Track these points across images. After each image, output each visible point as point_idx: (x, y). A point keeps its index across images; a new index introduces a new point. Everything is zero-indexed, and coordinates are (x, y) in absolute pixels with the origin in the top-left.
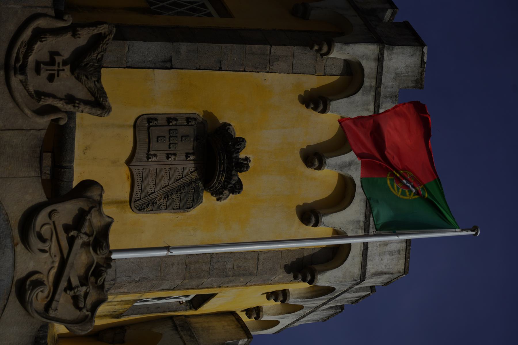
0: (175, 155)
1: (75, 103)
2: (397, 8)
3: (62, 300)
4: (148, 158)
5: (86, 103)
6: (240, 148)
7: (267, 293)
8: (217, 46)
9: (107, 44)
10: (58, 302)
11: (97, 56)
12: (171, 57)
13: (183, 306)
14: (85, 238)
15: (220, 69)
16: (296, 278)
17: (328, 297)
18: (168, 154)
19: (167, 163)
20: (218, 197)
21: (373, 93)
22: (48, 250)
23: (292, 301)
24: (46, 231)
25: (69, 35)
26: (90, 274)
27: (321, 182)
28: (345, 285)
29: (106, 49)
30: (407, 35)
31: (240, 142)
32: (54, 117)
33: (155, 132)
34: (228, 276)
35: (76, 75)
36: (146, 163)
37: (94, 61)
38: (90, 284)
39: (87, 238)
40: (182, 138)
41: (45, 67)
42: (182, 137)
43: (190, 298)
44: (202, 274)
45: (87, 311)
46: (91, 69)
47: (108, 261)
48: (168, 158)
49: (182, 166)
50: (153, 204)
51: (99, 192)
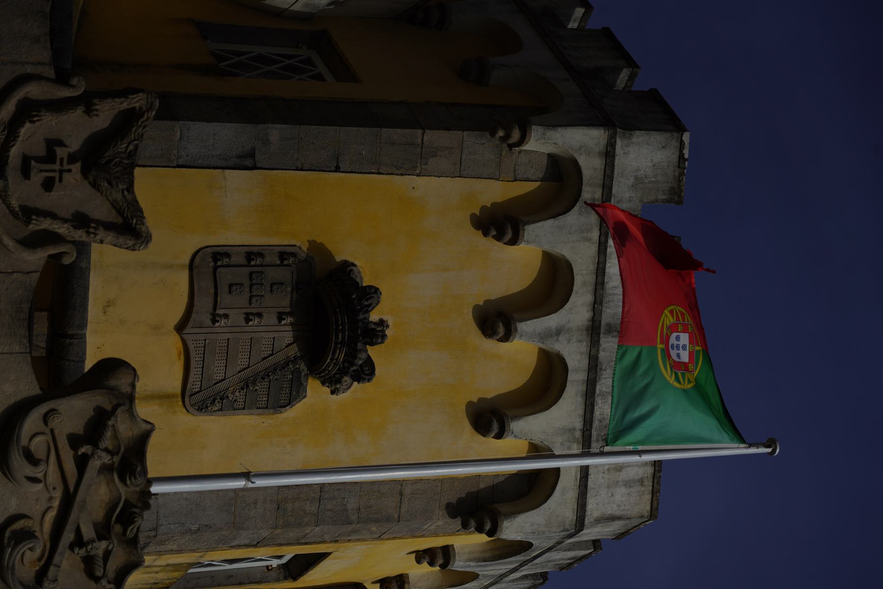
0: (260, 315)
1: (89, 227)
2: (638, 67)
3: (65, 565)
4: (214, 321)
5: (109, 227)
6: (370, 305)
7: (417, 552)
10: (59, 567)
11: (127, 147)
13: (272, 573)
14: (106, 459)
15: (337, 170)
16: (465, 526)
17: (521, 558)
18: (247, 314)
19: (246, 329)
20: (333, 387)
22: (42, 479)
23: (459, 565)
24: (38, 445)
25: (80, 111)
26: (114, 519)
27: (509, 363)
29: (142, 135)
31: (371, 294)
32: (53, 251)
33: (226, 276)
34: (350, 523)
35: (91, 179)
36: (209, 330)
37: (122, 155)
38: (113, 537)
39: (110, 457)
41: (38, 165)
42: (272, 285)
43: (284, 560)
44: (306, 520)
45: (109, 582)
46: (117, 169)
47: (146, 496)
48: (248, 320)
49: (272, 335)
50: (222, 399)
51: (129, 380)
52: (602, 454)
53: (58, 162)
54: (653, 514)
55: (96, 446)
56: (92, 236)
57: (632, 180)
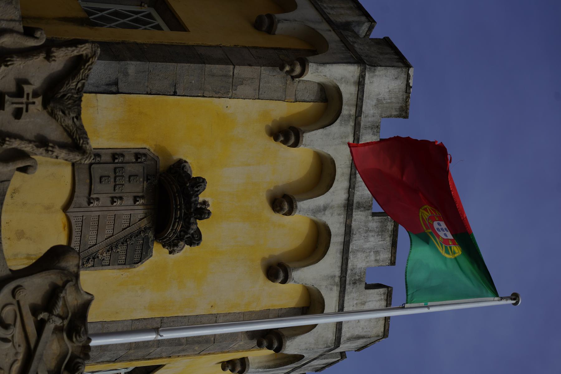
0: (121, 198)
1: (47, 146)
2: (375, 22)
4: (89, 203)
5: (62, 146)
6: (198, 191)
7: (223, 363)
8: (171, 66)
9: (90, 69)
11: (77, 85)
12: (117, 79)
14: (59, 322)
15: (175, 94)
18: (112, 198)
19: (111, 208)
20: (172, 249)
21: (352, 123)
22: (10, 339)
24: (8, 314)
25: (42, 56)
26: (63, 367)
27: (290, 231)
28: (316, 352)
29: (88, 75)
30: (389, 54)
31: (200, 183)
35: (49, 109)
37: (73, 91)
39: (61, 321)
40: (129, 179)
41: (10, 99)
43: (129, 370)
46: (70, 102)
47: (86, 348)
48: (113, 202)
49: (129, 212)
52: (403, 308)
53: (25, 96)
54: (385, 334)
55: (51, 312)
56: (50, 153)
57: (375, 102)
